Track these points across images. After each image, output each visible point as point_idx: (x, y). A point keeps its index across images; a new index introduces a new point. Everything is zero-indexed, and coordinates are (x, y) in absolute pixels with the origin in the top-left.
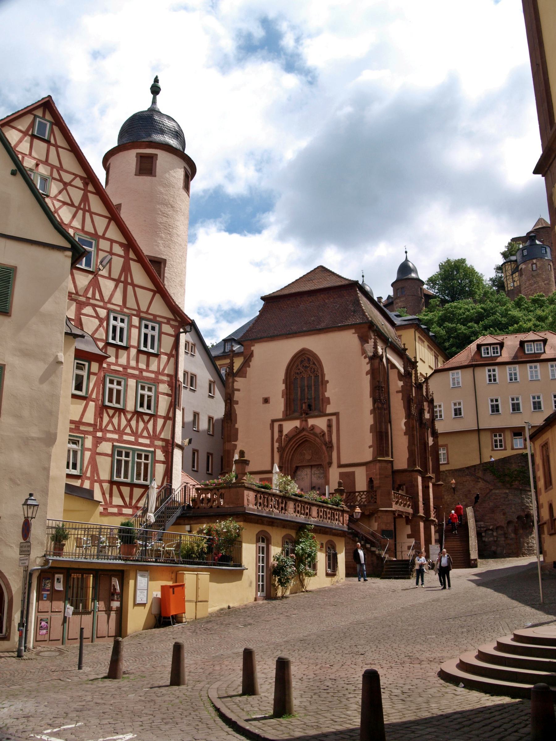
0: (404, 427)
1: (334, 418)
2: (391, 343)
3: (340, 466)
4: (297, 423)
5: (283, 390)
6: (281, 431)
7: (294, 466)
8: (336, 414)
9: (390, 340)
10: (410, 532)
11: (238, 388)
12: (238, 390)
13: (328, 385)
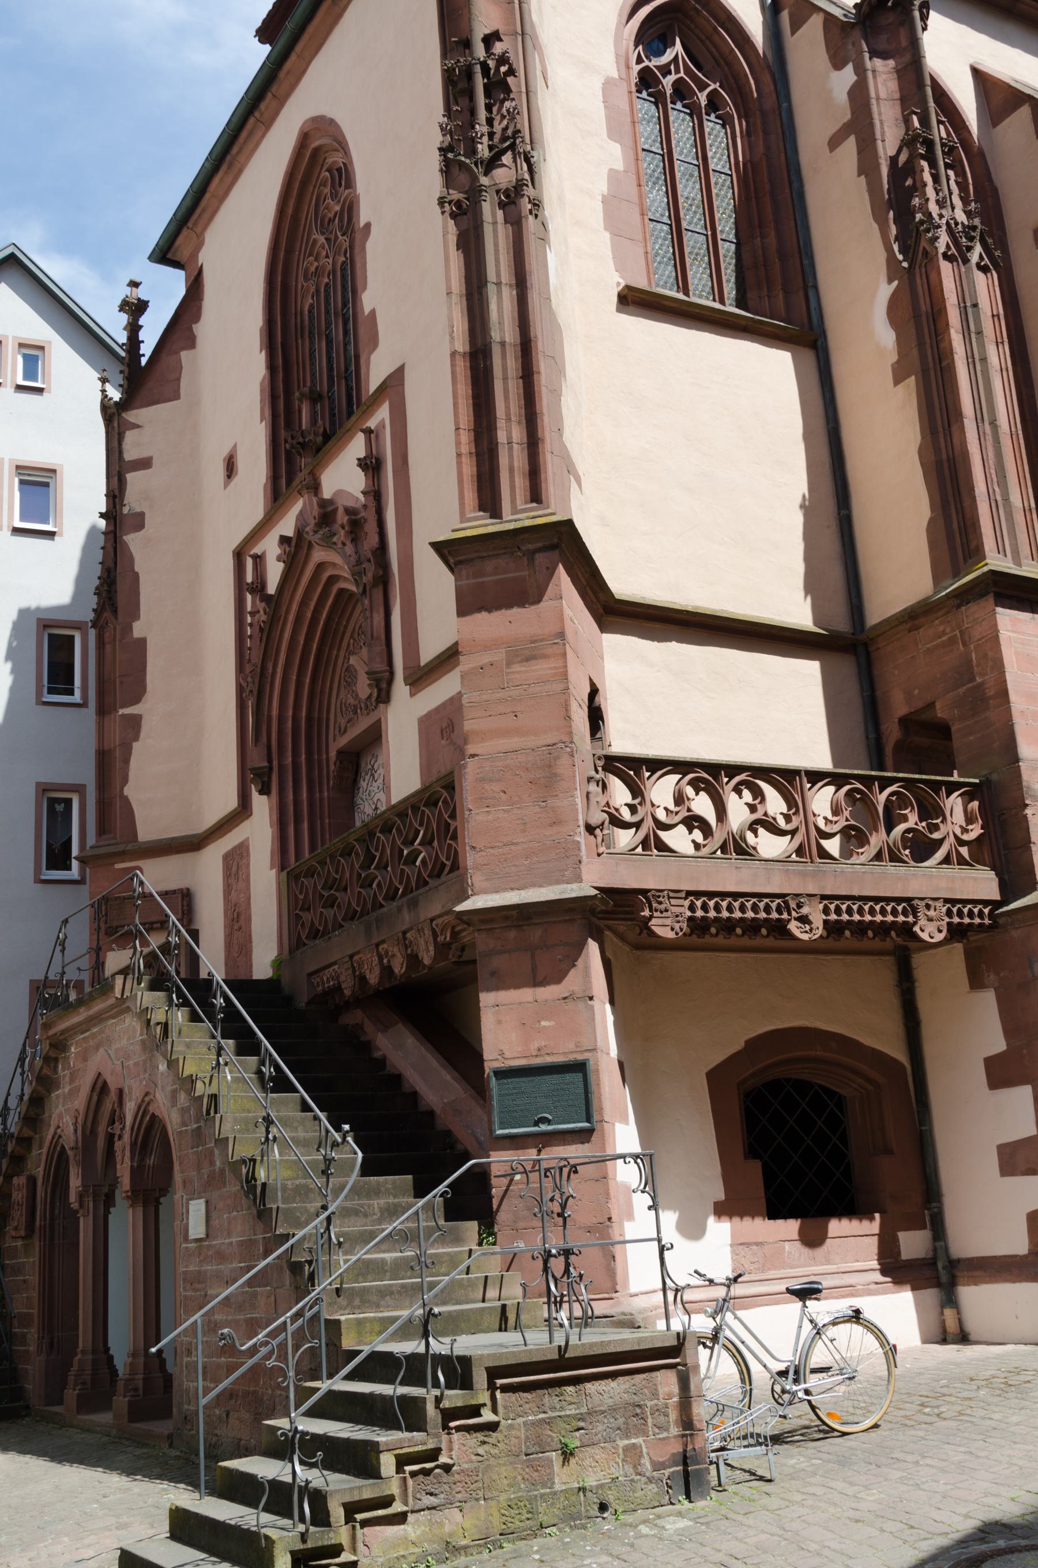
0: (886, 337)
6: (259, 587)
7: (333, 754)
8: (395, 382)
10: (999, 1045)
11: (145, 454)
12: (145, 464)
13: (370, 245)
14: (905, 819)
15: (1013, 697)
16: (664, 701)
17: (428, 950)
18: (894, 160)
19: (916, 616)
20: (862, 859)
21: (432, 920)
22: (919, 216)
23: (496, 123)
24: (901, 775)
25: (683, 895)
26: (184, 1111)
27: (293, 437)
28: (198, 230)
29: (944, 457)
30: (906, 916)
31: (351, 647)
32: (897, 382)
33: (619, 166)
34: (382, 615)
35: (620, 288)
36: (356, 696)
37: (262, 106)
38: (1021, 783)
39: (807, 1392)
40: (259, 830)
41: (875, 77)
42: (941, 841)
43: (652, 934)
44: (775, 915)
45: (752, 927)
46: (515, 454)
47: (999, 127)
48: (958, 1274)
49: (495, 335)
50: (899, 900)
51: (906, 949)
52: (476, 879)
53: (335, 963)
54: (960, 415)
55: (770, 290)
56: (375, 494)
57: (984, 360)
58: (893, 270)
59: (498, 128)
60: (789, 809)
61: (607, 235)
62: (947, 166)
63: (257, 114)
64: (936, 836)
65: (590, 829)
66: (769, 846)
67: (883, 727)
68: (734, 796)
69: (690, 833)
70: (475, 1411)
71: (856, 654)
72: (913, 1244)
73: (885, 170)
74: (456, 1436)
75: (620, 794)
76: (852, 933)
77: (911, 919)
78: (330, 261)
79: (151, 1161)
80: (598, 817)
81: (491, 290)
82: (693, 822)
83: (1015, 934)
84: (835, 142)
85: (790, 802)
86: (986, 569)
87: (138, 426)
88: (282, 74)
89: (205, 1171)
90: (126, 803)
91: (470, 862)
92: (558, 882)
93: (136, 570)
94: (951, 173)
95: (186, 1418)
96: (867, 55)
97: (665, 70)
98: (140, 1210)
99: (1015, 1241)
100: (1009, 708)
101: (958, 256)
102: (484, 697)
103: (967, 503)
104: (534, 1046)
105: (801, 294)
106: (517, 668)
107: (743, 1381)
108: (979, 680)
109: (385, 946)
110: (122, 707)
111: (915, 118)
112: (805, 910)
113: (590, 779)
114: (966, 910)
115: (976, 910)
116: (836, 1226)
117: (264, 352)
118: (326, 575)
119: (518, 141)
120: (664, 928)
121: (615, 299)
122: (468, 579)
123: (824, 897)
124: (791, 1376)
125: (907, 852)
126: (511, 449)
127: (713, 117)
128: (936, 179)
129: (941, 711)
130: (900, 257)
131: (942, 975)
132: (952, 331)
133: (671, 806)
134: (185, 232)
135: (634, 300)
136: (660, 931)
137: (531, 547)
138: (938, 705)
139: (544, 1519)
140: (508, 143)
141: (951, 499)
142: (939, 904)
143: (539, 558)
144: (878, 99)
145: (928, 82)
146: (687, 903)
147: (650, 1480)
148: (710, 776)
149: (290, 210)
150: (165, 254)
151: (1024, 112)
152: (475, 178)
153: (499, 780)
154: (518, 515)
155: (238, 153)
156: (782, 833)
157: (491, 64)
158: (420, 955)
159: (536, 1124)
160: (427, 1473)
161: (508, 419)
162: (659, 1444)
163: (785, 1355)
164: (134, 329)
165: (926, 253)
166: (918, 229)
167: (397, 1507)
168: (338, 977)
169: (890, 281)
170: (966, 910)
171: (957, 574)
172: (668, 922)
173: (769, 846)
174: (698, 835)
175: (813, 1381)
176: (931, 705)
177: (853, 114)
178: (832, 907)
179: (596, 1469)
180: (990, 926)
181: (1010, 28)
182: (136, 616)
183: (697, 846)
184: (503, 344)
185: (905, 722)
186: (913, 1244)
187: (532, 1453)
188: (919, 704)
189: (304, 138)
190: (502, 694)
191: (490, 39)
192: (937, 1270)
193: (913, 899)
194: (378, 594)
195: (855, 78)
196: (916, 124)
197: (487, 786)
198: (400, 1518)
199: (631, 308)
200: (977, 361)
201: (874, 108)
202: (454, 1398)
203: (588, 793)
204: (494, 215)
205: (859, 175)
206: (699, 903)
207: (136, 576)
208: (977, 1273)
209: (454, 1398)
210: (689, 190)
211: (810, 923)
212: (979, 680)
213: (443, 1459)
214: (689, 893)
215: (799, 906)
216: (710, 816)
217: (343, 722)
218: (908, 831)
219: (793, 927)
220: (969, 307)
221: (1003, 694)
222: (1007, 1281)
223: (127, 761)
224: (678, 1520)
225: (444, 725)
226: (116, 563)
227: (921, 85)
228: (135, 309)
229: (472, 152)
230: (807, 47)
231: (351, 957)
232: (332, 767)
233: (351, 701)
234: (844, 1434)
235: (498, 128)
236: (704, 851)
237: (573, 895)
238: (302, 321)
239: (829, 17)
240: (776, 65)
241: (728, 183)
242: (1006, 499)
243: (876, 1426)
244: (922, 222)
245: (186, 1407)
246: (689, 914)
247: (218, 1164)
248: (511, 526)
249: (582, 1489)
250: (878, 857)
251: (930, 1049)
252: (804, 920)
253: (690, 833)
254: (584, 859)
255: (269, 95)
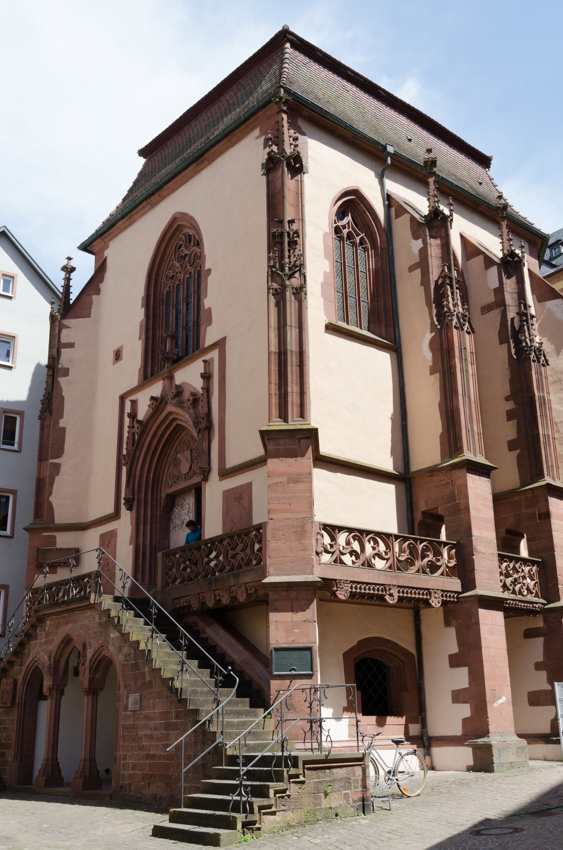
0: (428, 355)
1: (214, 355)
2: (395, 156)
3: (225, 474)
4: (156, 389)
5: (141, 322)
6: (133, 416)
7: (163, 496)
8: (221, 344)
9: (390, 149)
10: (455, 649)
11: (71, 341)
12: (71, 345)
13: (210, 279)
14: (428, 556)
15: (471, 510)
16: (340, 501)
17: (242, 596)
18: (436, 282)
19: (433, 471)
20: (412, 572)
21: (246, 584)
22: (446, 309)
23: (292, 258)
24: (428, 538)
25: (349, 582)
26: (127, 655)
27: (163, 354)
28: (106, 240)
29: (449, 408)
30: (427, 596)
31: (178, 449)
32: (431, 373)
33: (328, 270)
34: (207, 443)
35: (326, 322)
36: (179, 471)
37: (152, 198)
38: (472, 545)
39: (397, 780)
40: (125, 526)
41: (431, 247)
42: (440, 566)
43: (336, 596)
44: (380, 593)
45: (371, 596)
46: (294, 397)
47: (470, 261)
48: (432, 742)
49: (289, 347)
50: (425, 589)
51: (419, 607)
52: (270, 569)
53: (190, 596)
54: (457, 393)
55: (380, 325)
56: (207, 389)
57: (467, 371)
58: (433, 328)
59: (293, 260)
60: (387, 549)
61: (322, 299)
62: (457, 288)
63: (149, 201)
64: (439, 564)
65: (317, 553)
66: (379, 564)
67: (415, 514)
68: (368, 543)
69: (351, 557)
70: (297, 776)
71: (405, 482)
72: (415, 729)
73: (432, 287)
74: (292, 785)
75: (327, 540)
76: (406, 601)
77: (428, 597)
78: (182, 275)
79: (98, 676)
80: (320, 549)
81: (288, 328)
82: (352, 553)
83: (465, 605)
84: (411, 269)
85: (387, 547)
86: (464, 458)
87: (69, 327)
88: (165, 187)
89: (139, 682)
90: (50, 504)
91: (268, 562)
92: (304, 574)
93: (63, 394)
94: (458, 291)
95: (121, 787)
96: (428, 237)
97: (344, 227)
98: (91, 697)
99: (457, 730)
100: (470, 515)
101: (460, 327)
102: (277, 495)
103: (457, 429)
104: (290, 640)
105: (392, 329)
106: (291, 485)
107: (376, 774)
108: (458, 501)
109: (219, 591)
110: (51, 459)
111: (446, 267)
112: (392, 591)
113: (318, 533)
114: (448, 595)
115: (452, 595)
116: (390, 720)
117: (143, 309)
118: (171, 417)
119: (302, 268)
120: (342, 595)
121: (324, 327)
122: (273, 446)
123: (399, 586)
124: (392, 773)
125: (428, 570)
126: (293, 395)
127: (360, 248)
128: (452, 293)
129: (440, 511)
130: (437, 323)
131: (432, 619)
132: (456, 359)
133: (345, 546)
134: (99, 240)
135: (331, 328)
136: (339, 596)
137: (299, 436)
138: (439, 509)
139: (319, 818)
140: (297, 269)
141: (451, 425)
142: (439, 592)
143: (303, 441)
144: (431, 256)
145: (452, 253)
146: (350, 585)
147: (352, 806)
148: (360, 534)
149: (163, 248)
150: (86, 247)
151: (481, 257)
152: (283, 281)
153: (281, 530)
154: (295, 424)
155: (135, 214)
156: (383, 559)
157: (291, 233)
158: (238, 597)
159: (290, 671)
160: (283, 797)
161: (292, 383)
162: (355, 793)
163: (390, 766)
164: (68, 280)
165: (447, 325)
166: (445, 315)
167: (274, 809)
168: (190, 601)
169: (431, 332)
170: (448, 595)
171: (451, 457)
172: (343, 593)
173: (379, 564)
174: (354, 558)
175: (399, 776)
176: (437, 508)
177: (420, 260)
178: (401, 590)
179: (335, 801)
180: (457, 602)
181: (476, 217)
182: (61, 416)
183: (353, 563)
184: (292, 351)
185: (424, 513)
186: (415, 729)
187: (315, 793)
188: (432, 507)
189: (174, 219)
190: (284, 495)
191: (291, 222)
192: (423, 740)
193: (430, 589)
194: (206, 433)
195: (423, 245)
196: (446, 271)
197: (276, 532)
198: (274, 813)
199: (330, 331)
200: (464, 371)
201: (430, 260)
202: (293, 771)
203: (317, 539)
204: (290, 297)
205: (421, 285)
206: (354, 586)
207: (63, 398)
208: (439, 742)
209: (293, 771)
210: (350, 278)
211: (393, 596)
212: (458, 501)
213: (288, 793)
214: (351, 582)
215: (390, 589)
216: (359, 550)
217: (170, 483)
218: (429, 561)
219: (387, 597)
220: (462, 349)
221: (467, 509)
222: (453, 746)
223: (52, 484)
224: (364, 820)
225: (237, 496)
226: (53, 390)
227: (449, 254)
228: (69, 270)
229: (282, 269)
230: (402, 227)
231: (199, 594)
232: (163, 501)
233: (176, 473)
234: (409, 797)
235: (293, 260)
236: (356, 565)
237: (311, 580)
238: (163, 298)
239: (412, 218)
240: (388, 232)
241: (365, 276)
242: (472, 429)
243: (419, 795)
244: (447, 312)
245: (121, 782)
246: (350, 590)
247: (148, 679)
248: (292, 427)
249: (330, 808)
250: (418, 571)
251: (425, 649)
252: (391, 595)
253: (351, 557)
254: (315, 566)
255: (157, 194)
